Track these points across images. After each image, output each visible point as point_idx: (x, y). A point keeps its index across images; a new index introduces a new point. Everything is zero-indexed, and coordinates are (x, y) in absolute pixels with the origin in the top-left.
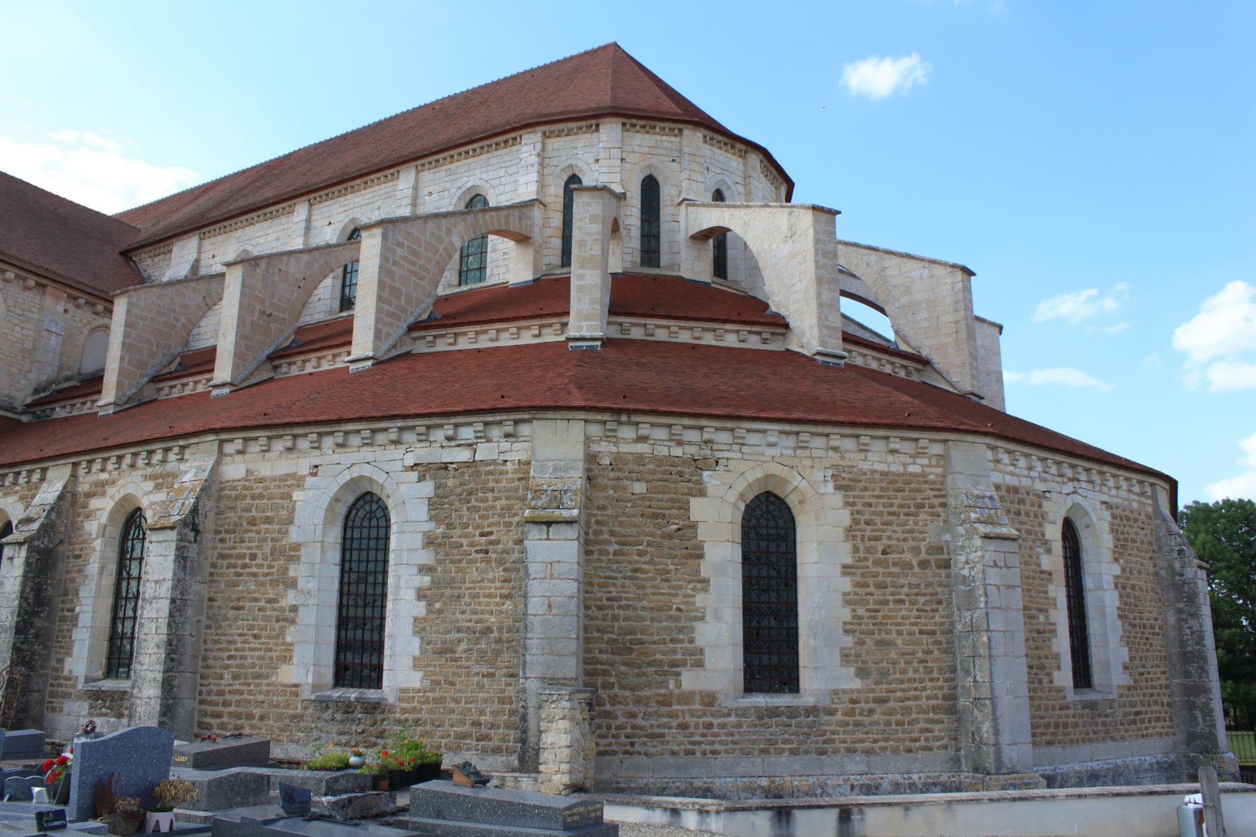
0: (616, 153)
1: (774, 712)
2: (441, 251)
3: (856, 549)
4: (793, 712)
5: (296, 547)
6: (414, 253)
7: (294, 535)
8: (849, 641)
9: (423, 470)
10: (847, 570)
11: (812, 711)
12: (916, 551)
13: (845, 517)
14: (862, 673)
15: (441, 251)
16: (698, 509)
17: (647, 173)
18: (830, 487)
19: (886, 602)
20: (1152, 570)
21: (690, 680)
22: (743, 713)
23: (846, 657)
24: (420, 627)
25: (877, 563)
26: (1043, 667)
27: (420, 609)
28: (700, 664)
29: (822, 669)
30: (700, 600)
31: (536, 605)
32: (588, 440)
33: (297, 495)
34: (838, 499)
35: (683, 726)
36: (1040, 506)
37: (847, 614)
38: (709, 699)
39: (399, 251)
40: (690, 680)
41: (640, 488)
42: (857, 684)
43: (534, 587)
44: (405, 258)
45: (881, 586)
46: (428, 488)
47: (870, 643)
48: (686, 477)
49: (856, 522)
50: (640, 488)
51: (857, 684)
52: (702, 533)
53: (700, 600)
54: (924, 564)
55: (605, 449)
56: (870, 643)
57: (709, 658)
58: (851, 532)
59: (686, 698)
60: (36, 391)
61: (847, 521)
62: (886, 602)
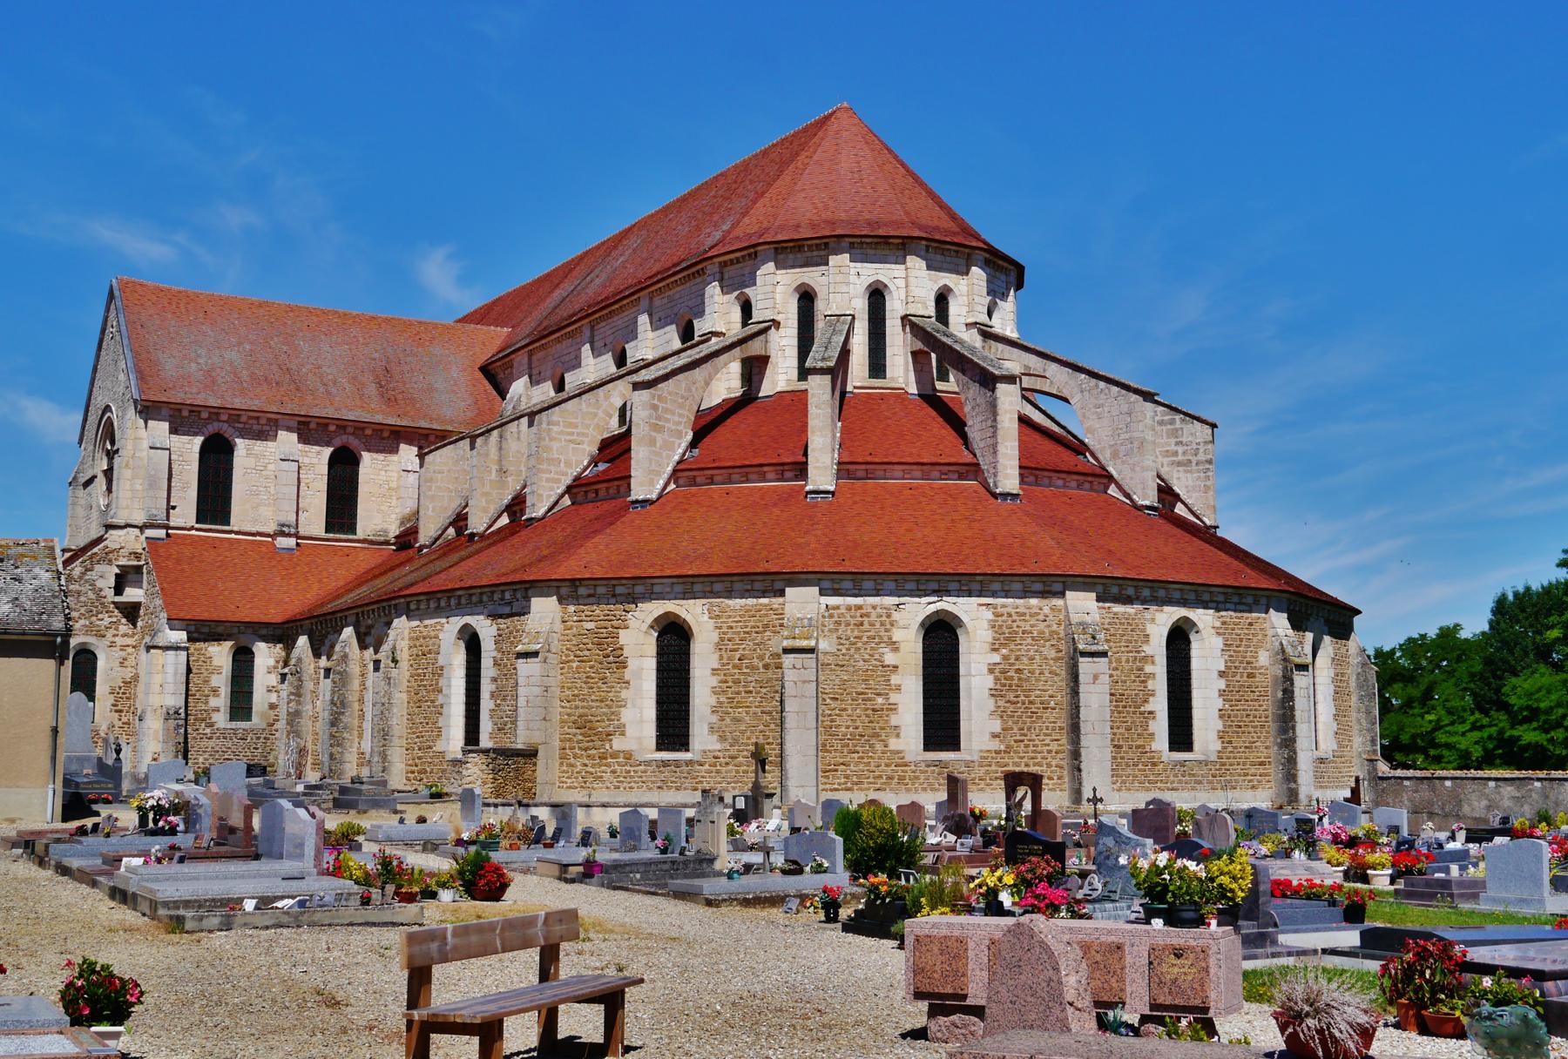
1: (665, 763)
2: (601, 414)
3: (721, 657)
4: (677, 763)
5: (442, 668)
6: (571, 425)
7: (441, 661)
8: (714, 719)
10: (1528, 589)
11: (689, 763)
12: (761, 658)
13: (715, 637)
14: (722, 739)
15: (601, 414)
16: (625, 637)
17: (797, 289)
18: (706, 618)
19: (738, 693)
21: (618, 744)
22: (648, 763)
23: (712, 729)
25: (735, 667)
26: (876, 735)
28: (623, 734)
30: (624, 694)
31: (522, 702)
33: (441, 636)
35: (614, 772)
36: (889, 616)
37: (713, 701)
38: (628, 756)
39: (555, 428)
40: (618, 744)
42: (718, 746)
43: (521, 691)
44: (561, 433)
45: (737, 682)
47: (728, 721)
49: (722, 639)
50: (591, 625)
52: (626, 653)
53: (624, 694)
54: (766, 667)
56: (728, 721)
57: (629, 732)
58: (719, 646)
59: (615, 755)
60: (402, 523)
61: (716, 639)
62: (738, 693)
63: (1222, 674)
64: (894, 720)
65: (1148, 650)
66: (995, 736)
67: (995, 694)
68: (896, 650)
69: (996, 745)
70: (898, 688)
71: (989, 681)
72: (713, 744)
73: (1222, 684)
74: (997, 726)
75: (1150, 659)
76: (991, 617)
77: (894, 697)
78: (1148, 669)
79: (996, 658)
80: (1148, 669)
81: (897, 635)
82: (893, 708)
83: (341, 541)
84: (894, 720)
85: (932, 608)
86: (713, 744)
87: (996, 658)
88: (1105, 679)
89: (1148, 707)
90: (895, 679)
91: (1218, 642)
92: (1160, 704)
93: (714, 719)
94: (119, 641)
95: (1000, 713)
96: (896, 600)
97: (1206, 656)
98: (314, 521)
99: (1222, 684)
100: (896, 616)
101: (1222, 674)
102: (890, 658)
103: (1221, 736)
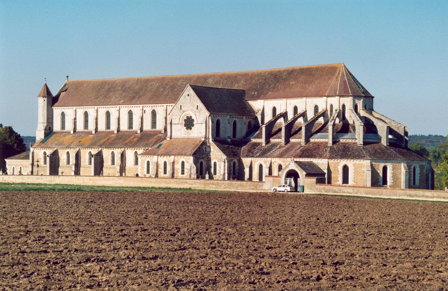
8: (353, 180)
13: (354, 168)
14: (355, 182)
23: (353, 181)
29: (351, 182)
34: (353, 166)
37: (353, 177)
51: (354, 183)
66: (392, 183)
68: (380, 170)
69: (392, 184)
72: (353, 183)
73: (419, 175)
74: (392, 181)
75: (411, 172)
76: (392, 165)
78: (411, 173)
79: (393, 172)
80: (411, 173)
85: (384, 165)
86: (353, 183)
88: (408, 175)
91: (419, 169)
94: (206, 160)
95: (393, 180)
96: (379, 163)
97: (418, 171)
98: (232, 137)
99: (419, 175)
100: (380, 165)
101: (419, 174)
103: (419, 183)
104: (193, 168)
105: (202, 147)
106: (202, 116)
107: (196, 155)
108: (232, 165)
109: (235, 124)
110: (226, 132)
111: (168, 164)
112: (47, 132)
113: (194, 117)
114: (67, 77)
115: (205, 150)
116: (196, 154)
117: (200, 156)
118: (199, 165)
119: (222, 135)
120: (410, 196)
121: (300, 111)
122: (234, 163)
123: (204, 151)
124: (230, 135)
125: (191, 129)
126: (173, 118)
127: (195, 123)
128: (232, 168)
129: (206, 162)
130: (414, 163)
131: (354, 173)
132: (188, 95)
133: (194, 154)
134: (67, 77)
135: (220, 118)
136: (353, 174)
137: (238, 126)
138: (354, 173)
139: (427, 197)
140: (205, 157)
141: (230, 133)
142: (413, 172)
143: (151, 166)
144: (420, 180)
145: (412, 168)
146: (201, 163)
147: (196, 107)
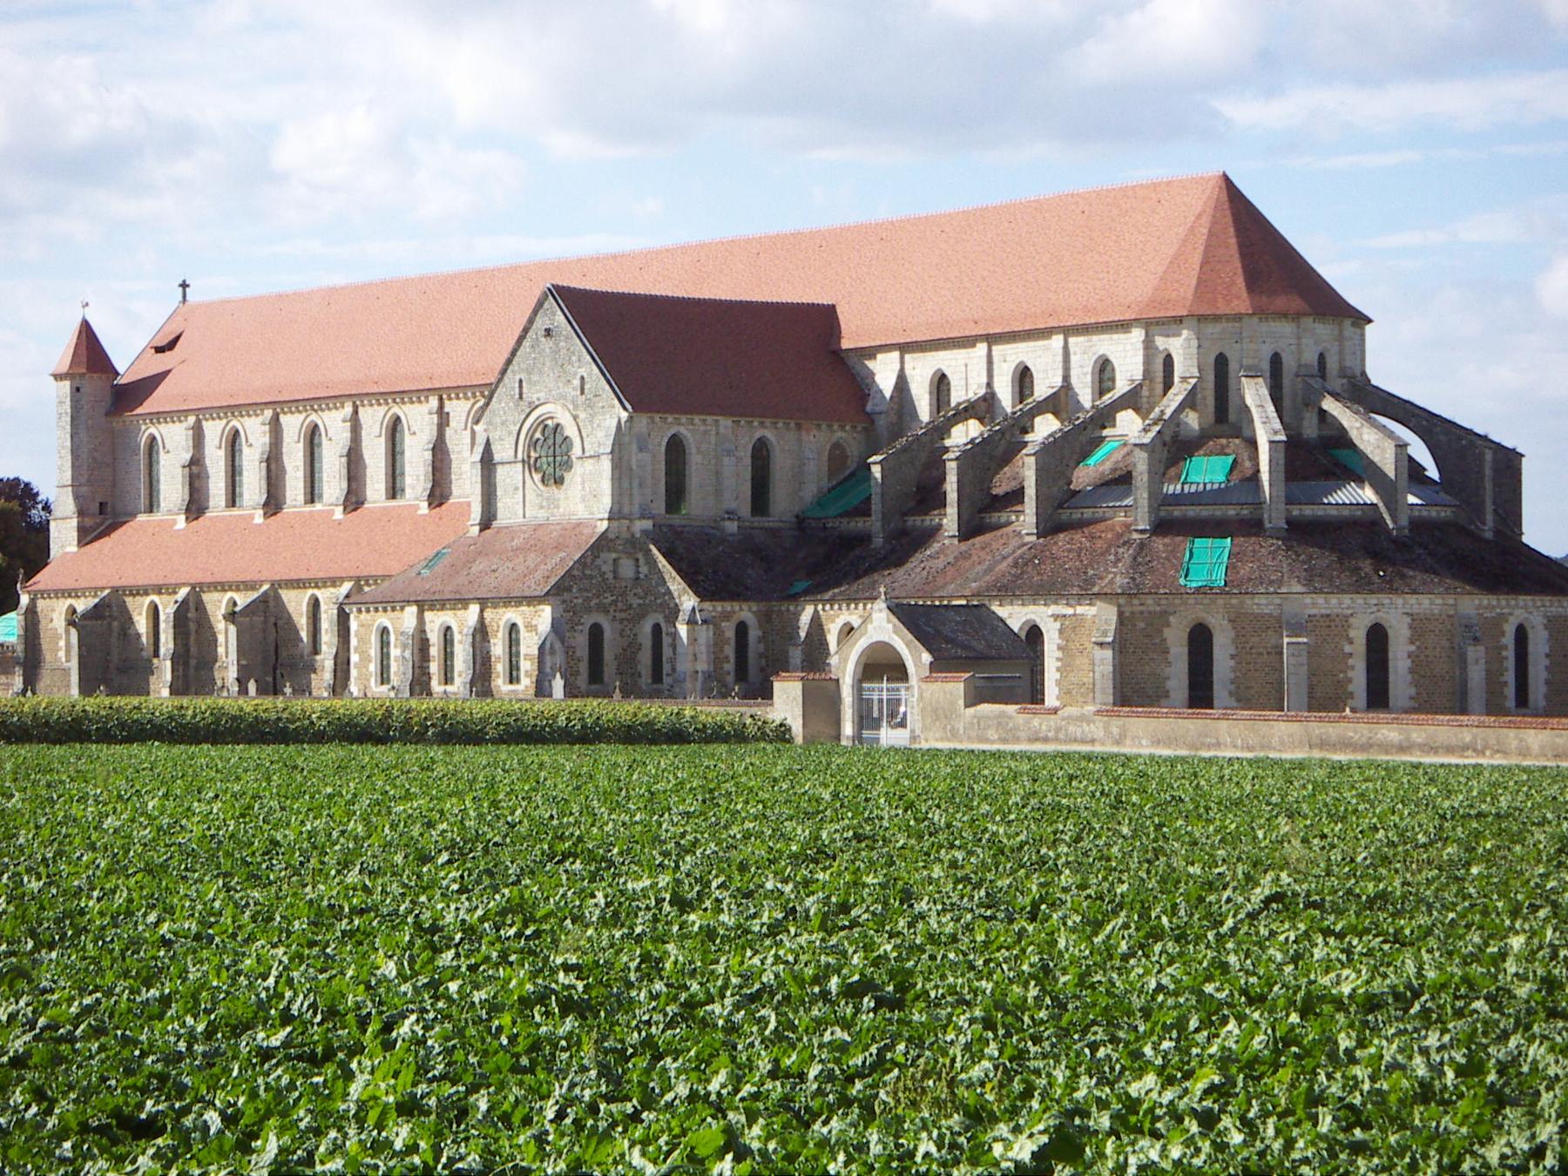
0: (1195, 343)
8: (1232, 687)
9: (1056, 617)
13: (1232, 634)
16: (1167, 632)
20: (1448, 644)
24: (1058, 683)
27: (1058, 676)
28: (1167, 697)
32: (1119, 606)
37: (1232, 676)
41: (1142, 625)
46: (1058, 625)
48: (1162, 619)
55: (1127, 611)
57: (1172, 694)
58: (1234, 641)
63: (1547, 656)
64: (1351, 688)
65: (1504, 641)
67: (1411, 671)
70: (1353, 668)
71: (1408, 663)
73: (1547, 662)
74: (1413, 691)
75: (1505, 647)
76: (1409, 620)
77: (1350, 674)
78: (1504, 653)
79: (1413, 648)
80: (1504, 653)
81: (1352, 633)
82: (1350, 681)
83: (759, 521)
84: (1351, 688)
87: (1413, 648)
89: (1504, 679)
90: (1351, 662)
92: (1510, 677)
93: (1232, 687)
98: (745, 510)
99: (1547, 662)
100: (1352, 620)
101: (1547, 656)
102: (1348, 649)
103: (1546, 696)
104: (553, 652)
105: (598, 562)
106: (595, 417)
107: (566, 596)
108: (730, 633)
109: (761, 455)
110: (718, 490)
111: (457, 637)
112: (89, 522)
113: (570, 431)
114: (184, 285)
115: (615, 572)
116: (569, 589)
117: (588, 599)
118: (581, 641)
119: (698, 504)
120: (1323, 744)
121: (1043, 387)
122: (742, 629)
123: (610, 576)
124: (733, 505)
125: (559, 481)
126: (494, 436)
127: (576, 451)
128: (730, 651)
129: (618, 626)
130: (1517, 606)
131: (1233, 657)
132: (548, 332)
133: (558, 592)
134: (184, 285)
135: (682, 430)
136: (1232, 663)
137: (781, 465)
138: (1233, 657)
139: (1386, 747)
140: (614, 602)
141: (738, 493)
142: (1511, 646)
143: (395, 652)
144: (1547, 682)
145: (1510, 629)
146: (596, 633)
147: (577, 382)
